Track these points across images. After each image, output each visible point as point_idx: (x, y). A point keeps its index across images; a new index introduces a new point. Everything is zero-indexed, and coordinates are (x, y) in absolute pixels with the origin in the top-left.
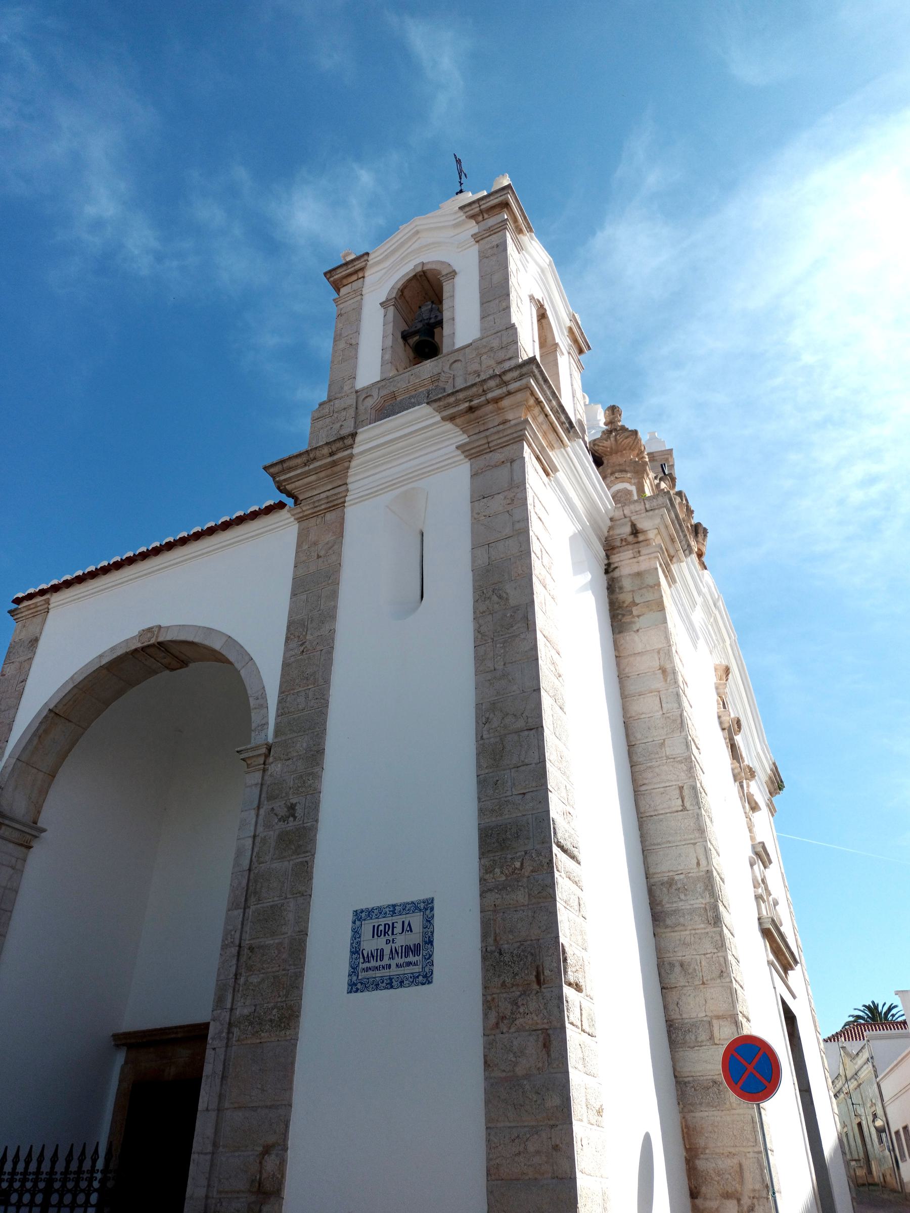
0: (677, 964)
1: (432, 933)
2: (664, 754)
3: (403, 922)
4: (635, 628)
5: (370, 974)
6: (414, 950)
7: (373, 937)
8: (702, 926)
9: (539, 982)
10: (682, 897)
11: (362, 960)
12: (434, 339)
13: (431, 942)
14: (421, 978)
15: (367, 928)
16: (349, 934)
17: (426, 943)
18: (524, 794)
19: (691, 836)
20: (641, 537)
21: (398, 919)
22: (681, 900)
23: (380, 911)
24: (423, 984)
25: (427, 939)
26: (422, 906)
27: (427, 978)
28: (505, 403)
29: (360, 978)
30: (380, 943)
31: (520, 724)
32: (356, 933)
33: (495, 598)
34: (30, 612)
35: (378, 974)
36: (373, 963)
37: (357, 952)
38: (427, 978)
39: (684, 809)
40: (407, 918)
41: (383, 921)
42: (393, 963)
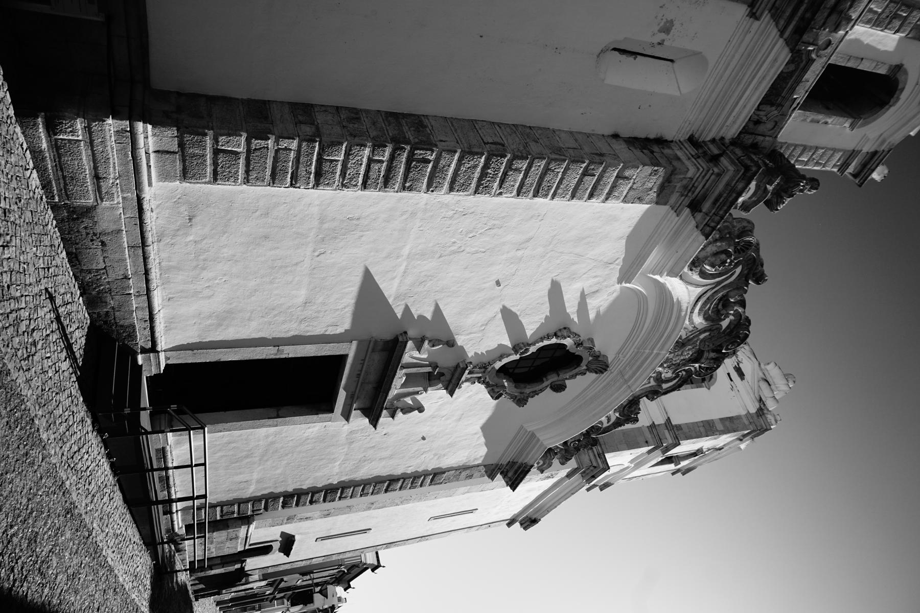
0: (357, 116)
2: (528, 141)
8: (391, 134)
10: (412, 129)
19: (464, 141)
22: (409, 128)
39: (485, 143)
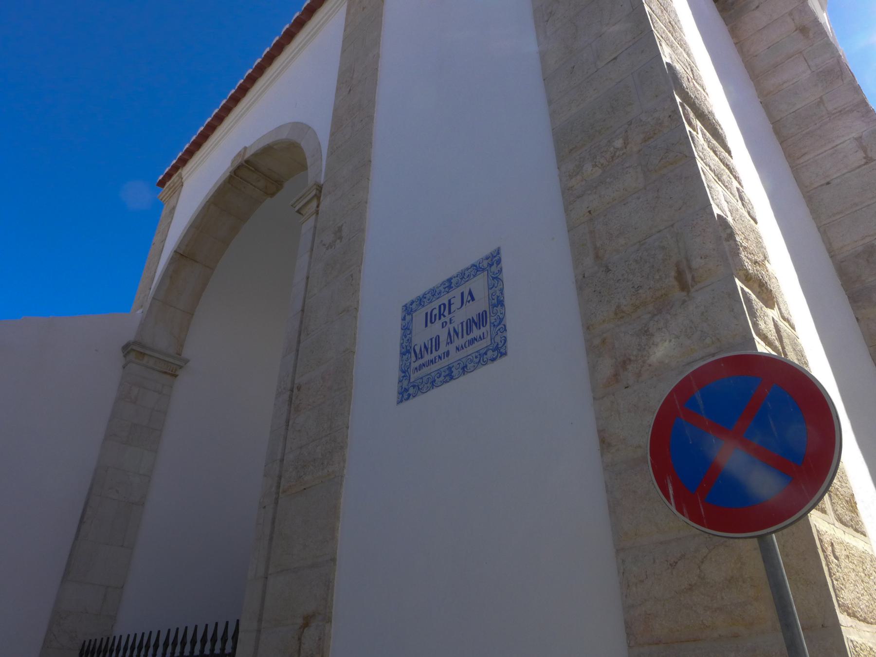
1: (502, 290)
3: (462, 294)
5: (425, 370)
6: (481, 320)
7: (426, 326)
9: (684, 287)
11: (414, 358)
13: (501, 303)
14: (490, 353)
15: (419, 317)
16: (399, 332)
17: (494, 306)
18: (615, 58)
21: (456, 293)
24: (493, 360)
25: (495, 301)
26: (485, 264)
29: (412, 380)
30: (436, 329)
32: (406, 329)
34: (171, 190)
35: (434, 367)
36: (427, 357)
37: (408, 352)
38: (499, 351)
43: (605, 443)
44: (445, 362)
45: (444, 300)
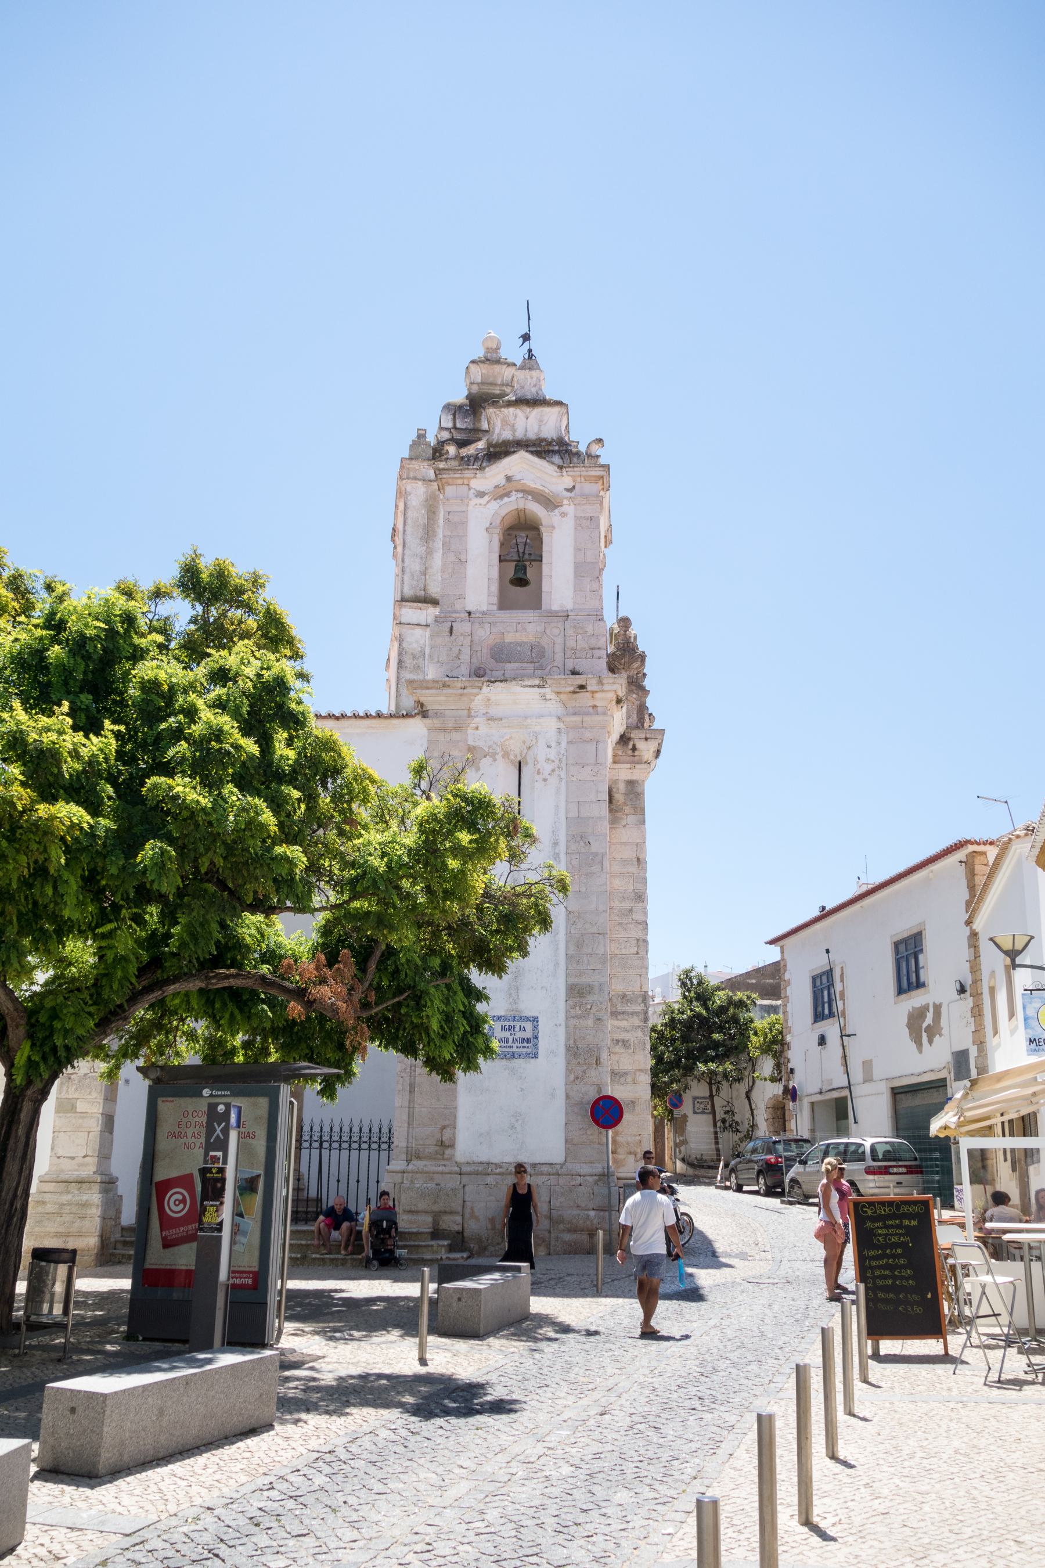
4: (624, 823)
6: (528, 1041)
12: (525, 573)
13: (537, 1038)
20: (637, 753)
21: (517, 1024)
23: (506, 1018)
27: (535, 1056)
28: (597, 695)
30: (507, 1034)
31: (594, 930)
33: (582, 843)
38: (535, 1056)
40: (523, 1024)
41: (507, 1024)
42: (515, 1046)
43: (567, 1097)
44: (511, 1050)
45: (512, 1024)
